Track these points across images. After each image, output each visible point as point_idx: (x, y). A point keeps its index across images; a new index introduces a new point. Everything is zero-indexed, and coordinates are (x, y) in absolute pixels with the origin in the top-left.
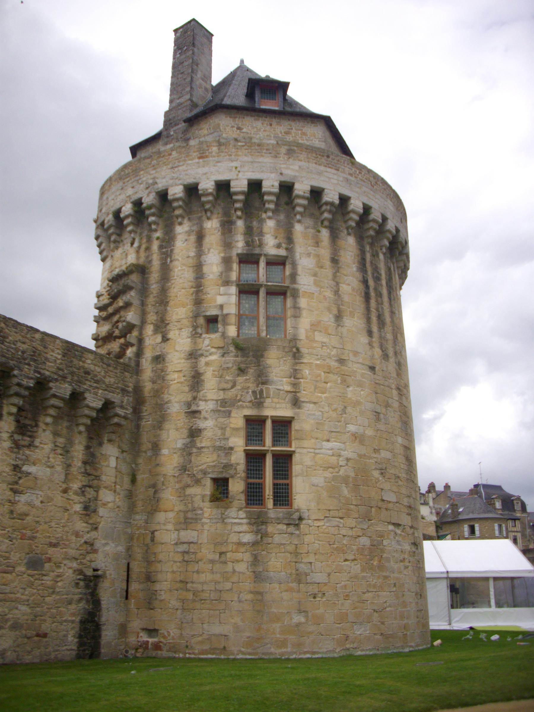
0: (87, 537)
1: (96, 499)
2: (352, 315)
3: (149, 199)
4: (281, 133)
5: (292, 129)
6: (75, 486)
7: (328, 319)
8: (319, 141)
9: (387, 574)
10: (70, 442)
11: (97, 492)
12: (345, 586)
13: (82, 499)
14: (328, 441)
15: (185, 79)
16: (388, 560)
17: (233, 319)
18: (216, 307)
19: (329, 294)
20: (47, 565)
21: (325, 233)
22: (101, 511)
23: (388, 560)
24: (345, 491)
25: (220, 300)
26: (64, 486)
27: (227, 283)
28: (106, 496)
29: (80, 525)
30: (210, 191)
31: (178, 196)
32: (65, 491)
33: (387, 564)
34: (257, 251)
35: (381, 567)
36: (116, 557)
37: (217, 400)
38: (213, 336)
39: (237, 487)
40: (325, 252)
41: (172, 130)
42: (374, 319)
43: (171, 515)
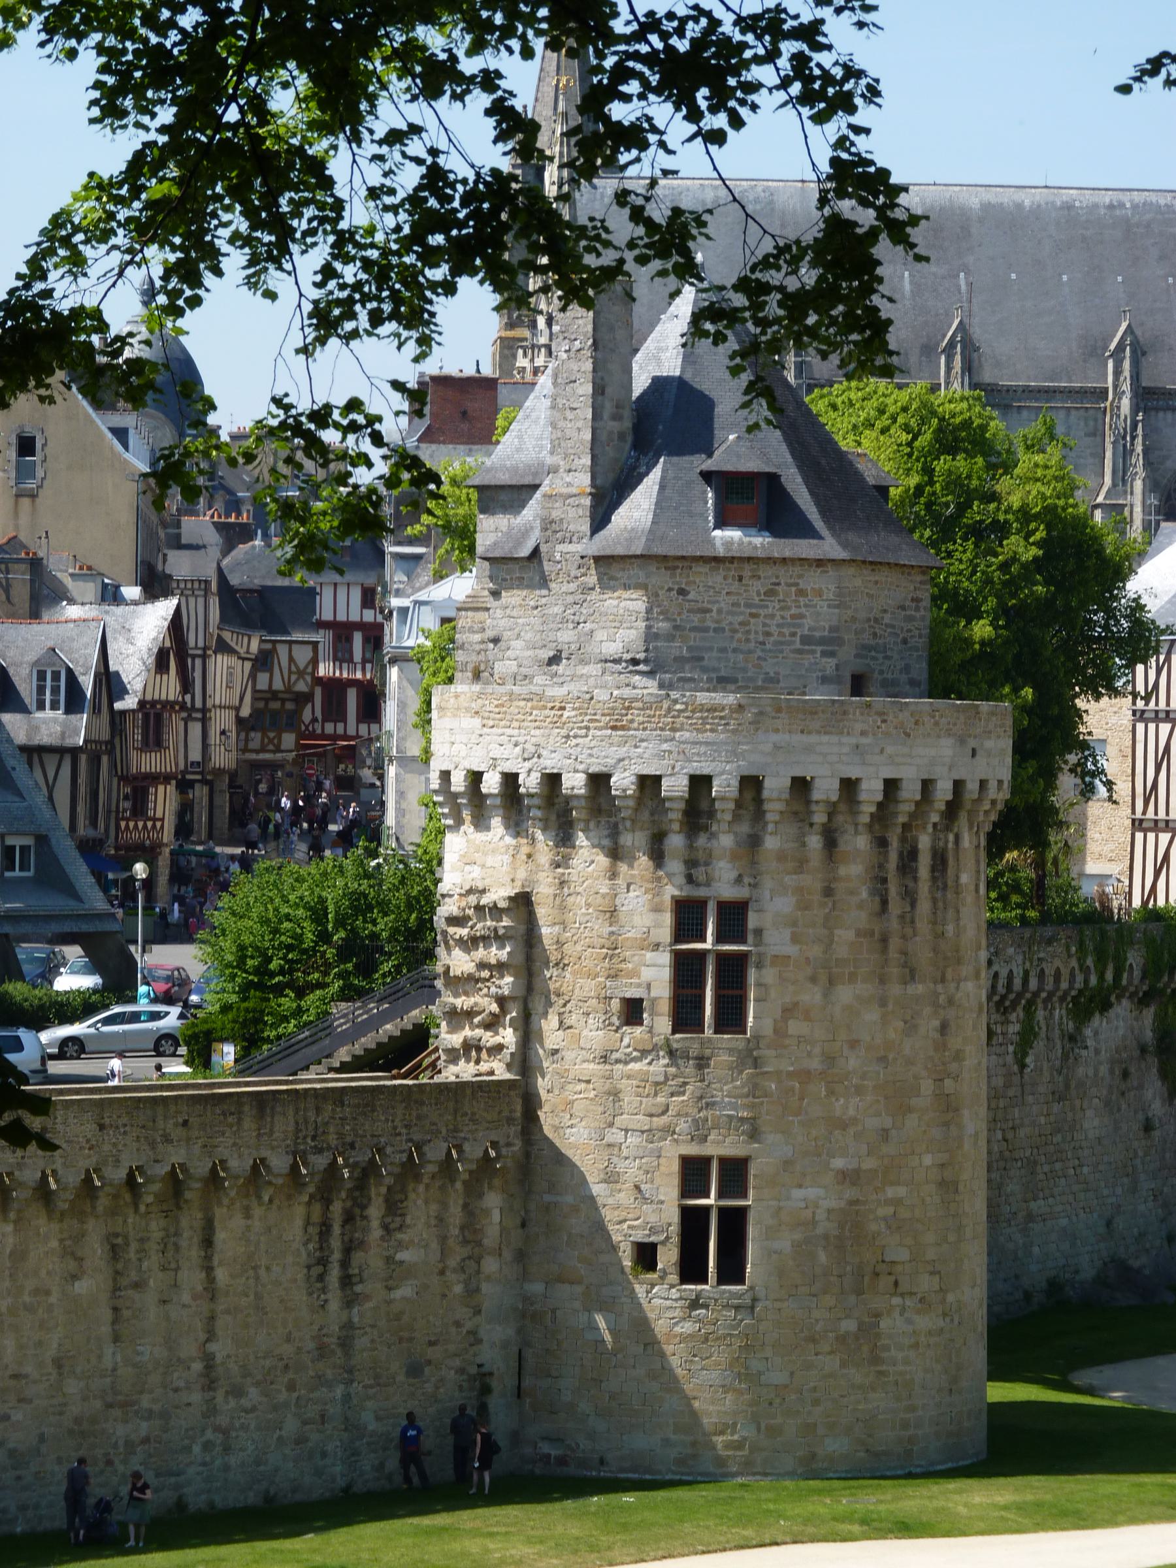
0: (469, 1325)
1: (478, 1272)
2: (852, 978)
3: (530, 783)
4: (759, 594)
5: (778, 584)
6: (452, 1262)
7: (812, 996)
8: (829, 606)
9: (884, 1368)
10: (444, 1205)
11: (479, 1263)
12: (815, 1388)
13: (462, 1277)
14: (800, 1186)
15: (579, 429)
16: (886, 1348)
17: (665, 1006)
18: (639, 985)
19: (816, 951)
20: (427, 1370)
21: (815, 842)
22: (485, 1287)
23: (886, 1348)
24: (822, 1257)
25: (647, 974)
26: (440, 1265)
27: (656, 946)
28: (490, 1265)
29: (462, 1313)
30: (629, 792)
31: (576, 791)
32: (442, 1273)
33: (885, 1355)
34: (701, 892)
35: (875, 1360)
36: (505, 1345)
37: (643, 1132)
38: (638, 1030)
39: (668, 1257)
40: (812, 881)
41: (559, 547)
42: (894, 971)
43: (579, 1289)
